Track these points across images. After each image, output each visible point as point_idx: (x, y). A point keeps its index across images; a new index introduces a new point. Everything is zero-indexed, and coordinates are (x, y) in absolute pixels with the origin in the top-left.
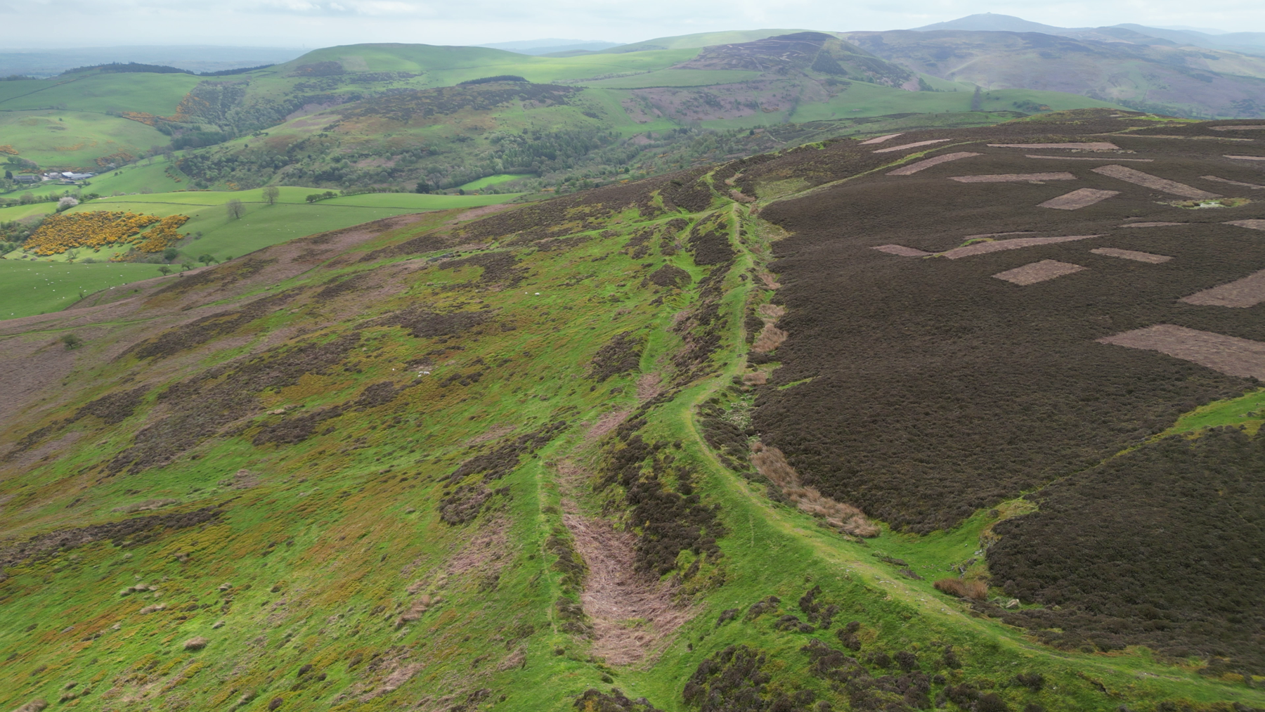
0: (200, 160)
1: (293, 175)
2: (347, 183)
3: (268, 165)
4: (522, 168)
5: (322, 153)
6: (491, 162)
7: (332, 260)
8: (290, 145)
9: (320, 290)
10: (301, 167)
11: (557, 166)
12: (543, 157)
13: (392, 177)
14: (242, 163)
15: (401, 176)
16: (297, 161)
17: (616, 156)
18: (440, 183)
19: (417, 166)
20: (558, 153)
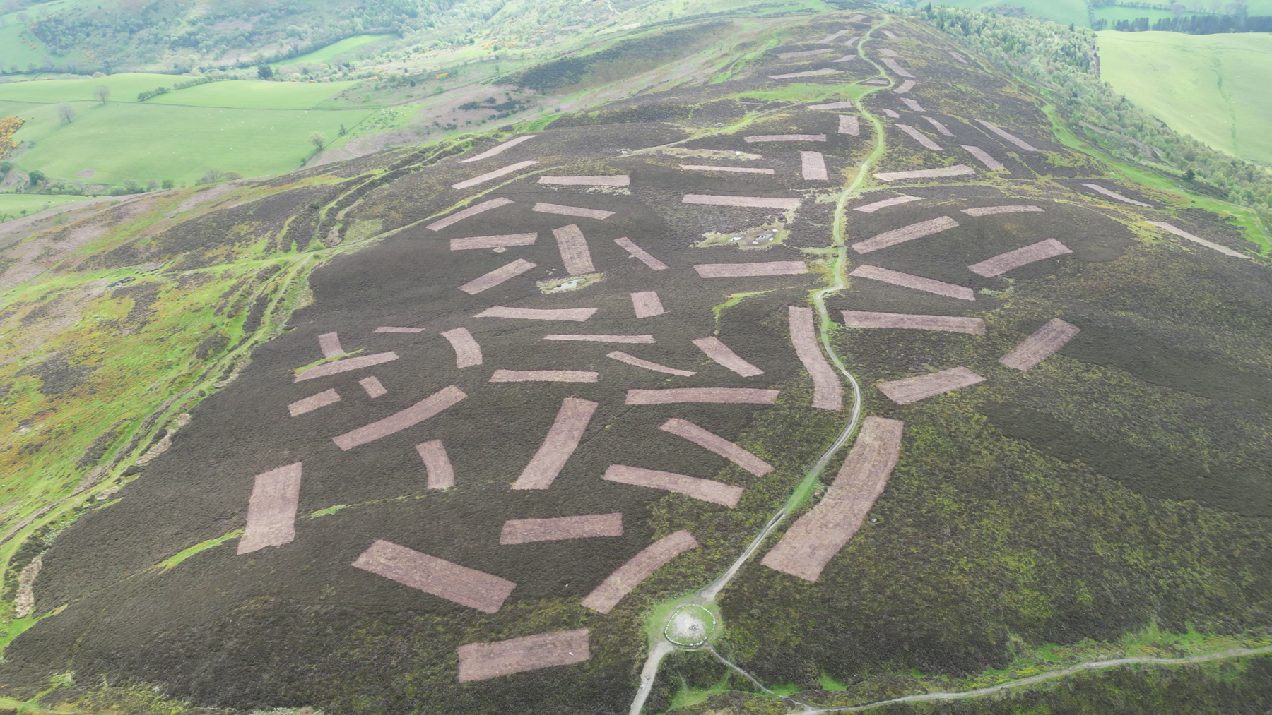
0: (53, 24)
1: (148, 41)
2: (204, 50)
3: (123, 30)
4: (381, 28)
5: (177, 14)
6: (352, 22)
7: (60, 263)
8: (144, 7)
9: (29, 309)
10: (156, 31)
11: (418, 25)
12: (404, 16)
13: (251, 42)
14: (97, 28)
15: (259, 40)
16: (152, 25)
17: (480, 10)
18: (299, 48)
19: (275, 28)
20: (420, 9)
